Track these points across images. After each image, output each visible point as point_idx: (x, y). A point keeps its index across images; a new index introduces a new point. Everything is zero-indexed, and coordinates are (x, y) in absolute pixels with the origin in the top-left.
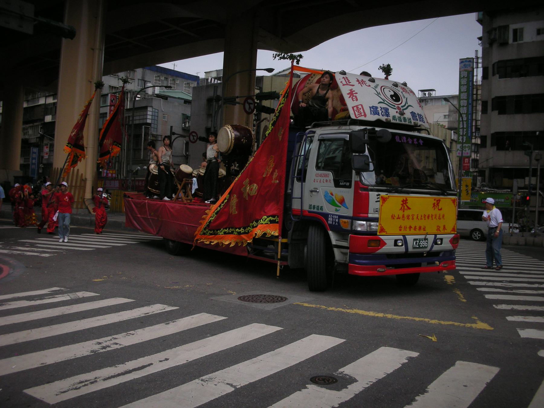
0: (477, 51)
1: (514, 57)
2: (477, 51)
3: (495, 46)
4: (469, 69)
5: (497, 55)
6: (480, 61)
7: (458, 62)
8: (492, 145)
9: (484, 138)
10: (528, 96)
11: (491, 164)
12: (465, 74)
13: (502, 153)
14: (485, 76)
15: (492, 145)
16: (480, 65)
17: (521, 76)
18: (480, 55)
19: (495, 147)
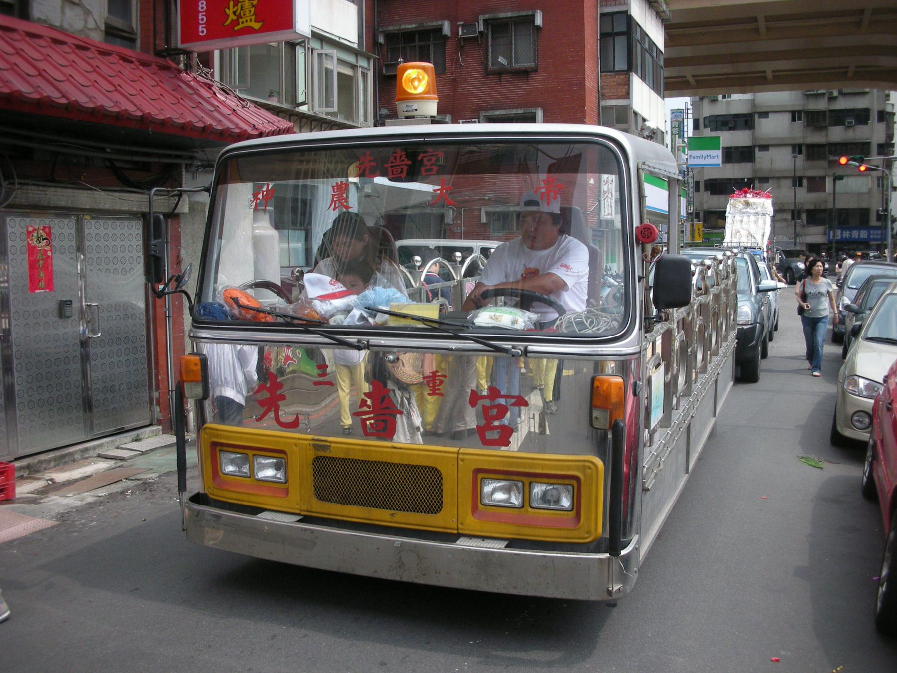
0: (686, 103)
1: (723, 113)
2: (686, 103)
3: (706, 102)
4: (681, 120)
5: (708, 110)
6: (690, 111)
7: (669, 112)
8: (706, 189)
9: (697, 184)
10: (737, 148)
11: (706, 207)
12: (677, 124)
13: (715, 197)
14: (696, 126)
15: (706, 189)
16: (690, 116)
17: (730, 129)
18: (690, 107)
19: (709, 193)
